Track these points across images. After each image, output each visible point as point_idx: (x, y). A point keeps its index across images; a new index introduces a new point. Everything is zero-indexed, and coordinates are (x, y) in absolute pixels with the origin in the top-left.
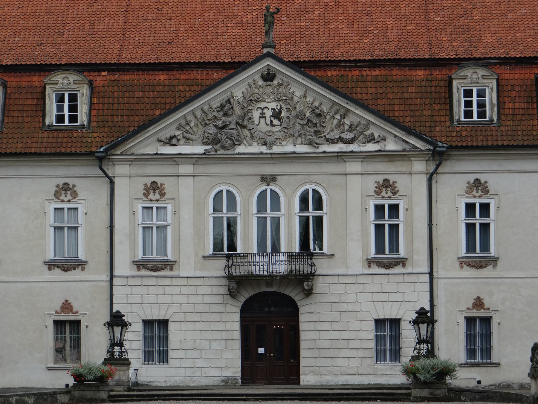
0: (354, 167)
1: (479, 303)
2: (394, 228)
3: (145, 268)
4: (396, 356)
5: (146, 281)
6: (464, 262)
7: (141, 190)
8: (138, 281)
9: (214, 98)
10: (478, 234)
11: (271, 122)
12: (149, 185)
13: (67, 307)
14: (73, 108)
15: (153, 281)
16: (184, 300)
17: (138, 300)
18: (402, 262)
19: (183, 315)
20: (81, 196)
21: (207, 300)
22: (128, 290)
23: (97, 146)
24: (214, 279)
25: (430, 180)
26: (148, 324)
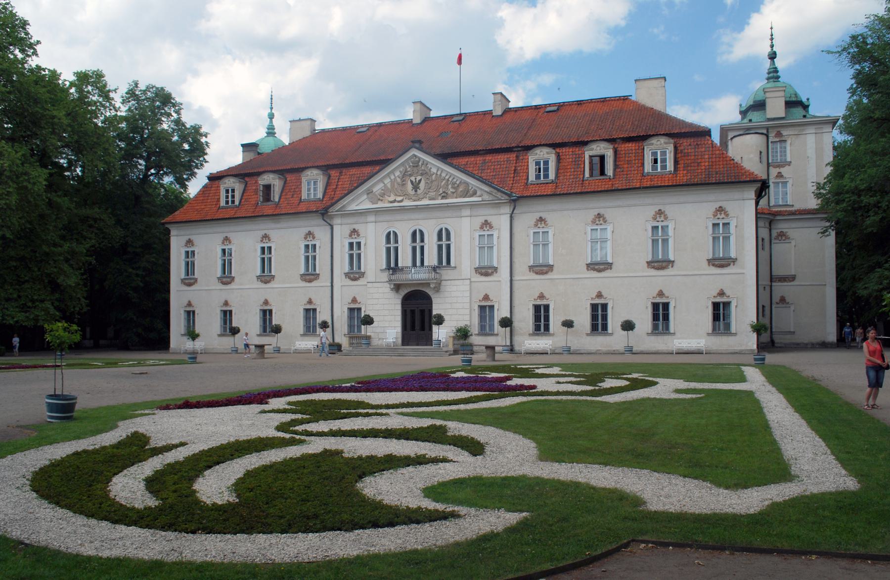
0: (466, 212)
7: (348, 232)
25: (511, 217)
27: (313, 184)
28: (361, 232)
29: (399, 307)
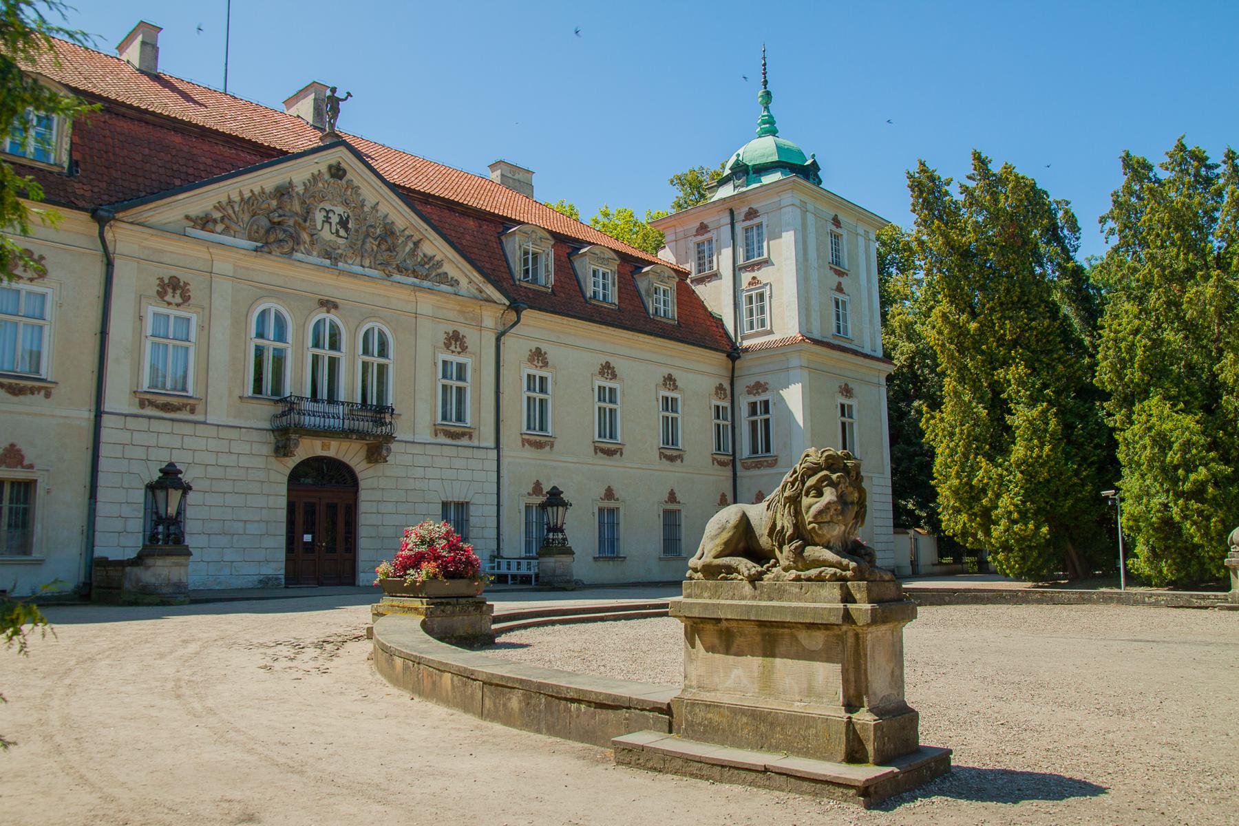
3: (152, 404)
5: (156, 426)
8: (143, 424)
11: (337, 231)
12: (166, 281)
15: (165, 427)
16: (210, 459)
17: (140, 453)
19: (208, 482)
20: (54, 273)
21: (244, 461)
22: (125, 437)
24: (255, 432)
25: (498, 340)
28: (195, 292)
29: (284, 489)
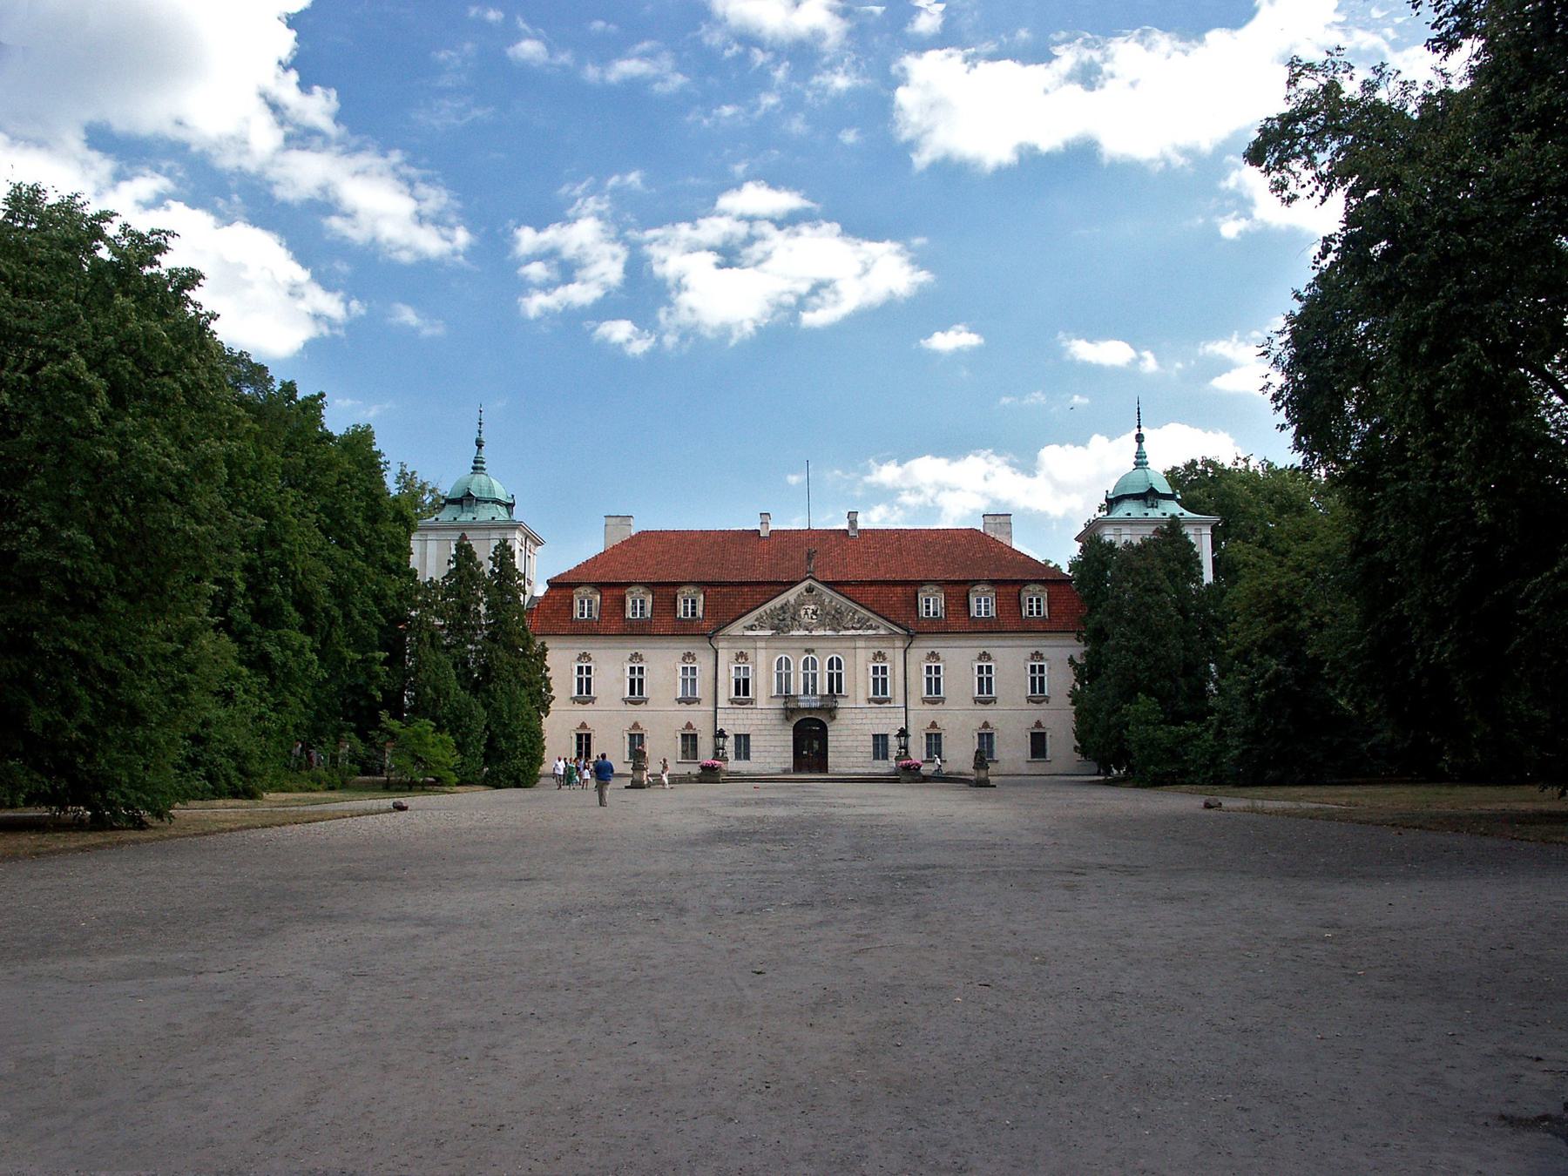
0: (860, 644)
1: (934, 725)
2: (884, 680)
4: (885, 757)
6: (924, 701)
9: (777, 602)
10: (934, 685)
13: (689, 726)
14: (694, 608)
18: (889, 700)
23: (708, 630)
26: (737, 736)
27: (690, 602)
